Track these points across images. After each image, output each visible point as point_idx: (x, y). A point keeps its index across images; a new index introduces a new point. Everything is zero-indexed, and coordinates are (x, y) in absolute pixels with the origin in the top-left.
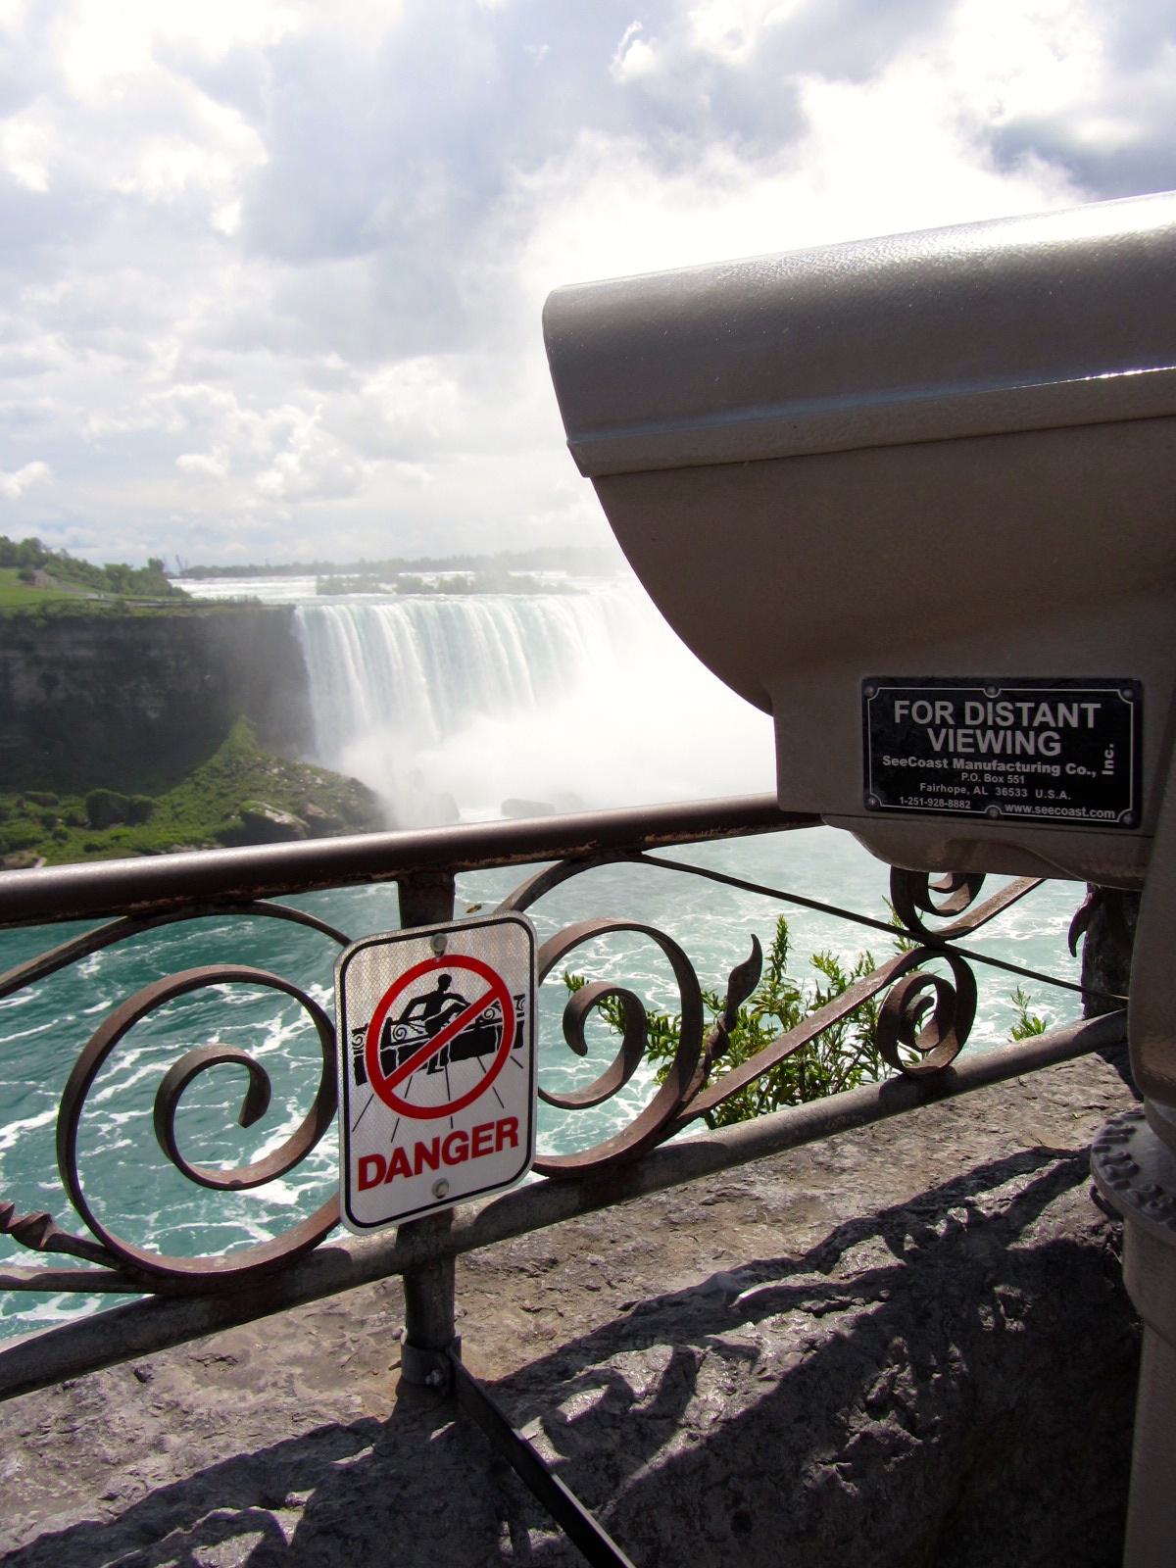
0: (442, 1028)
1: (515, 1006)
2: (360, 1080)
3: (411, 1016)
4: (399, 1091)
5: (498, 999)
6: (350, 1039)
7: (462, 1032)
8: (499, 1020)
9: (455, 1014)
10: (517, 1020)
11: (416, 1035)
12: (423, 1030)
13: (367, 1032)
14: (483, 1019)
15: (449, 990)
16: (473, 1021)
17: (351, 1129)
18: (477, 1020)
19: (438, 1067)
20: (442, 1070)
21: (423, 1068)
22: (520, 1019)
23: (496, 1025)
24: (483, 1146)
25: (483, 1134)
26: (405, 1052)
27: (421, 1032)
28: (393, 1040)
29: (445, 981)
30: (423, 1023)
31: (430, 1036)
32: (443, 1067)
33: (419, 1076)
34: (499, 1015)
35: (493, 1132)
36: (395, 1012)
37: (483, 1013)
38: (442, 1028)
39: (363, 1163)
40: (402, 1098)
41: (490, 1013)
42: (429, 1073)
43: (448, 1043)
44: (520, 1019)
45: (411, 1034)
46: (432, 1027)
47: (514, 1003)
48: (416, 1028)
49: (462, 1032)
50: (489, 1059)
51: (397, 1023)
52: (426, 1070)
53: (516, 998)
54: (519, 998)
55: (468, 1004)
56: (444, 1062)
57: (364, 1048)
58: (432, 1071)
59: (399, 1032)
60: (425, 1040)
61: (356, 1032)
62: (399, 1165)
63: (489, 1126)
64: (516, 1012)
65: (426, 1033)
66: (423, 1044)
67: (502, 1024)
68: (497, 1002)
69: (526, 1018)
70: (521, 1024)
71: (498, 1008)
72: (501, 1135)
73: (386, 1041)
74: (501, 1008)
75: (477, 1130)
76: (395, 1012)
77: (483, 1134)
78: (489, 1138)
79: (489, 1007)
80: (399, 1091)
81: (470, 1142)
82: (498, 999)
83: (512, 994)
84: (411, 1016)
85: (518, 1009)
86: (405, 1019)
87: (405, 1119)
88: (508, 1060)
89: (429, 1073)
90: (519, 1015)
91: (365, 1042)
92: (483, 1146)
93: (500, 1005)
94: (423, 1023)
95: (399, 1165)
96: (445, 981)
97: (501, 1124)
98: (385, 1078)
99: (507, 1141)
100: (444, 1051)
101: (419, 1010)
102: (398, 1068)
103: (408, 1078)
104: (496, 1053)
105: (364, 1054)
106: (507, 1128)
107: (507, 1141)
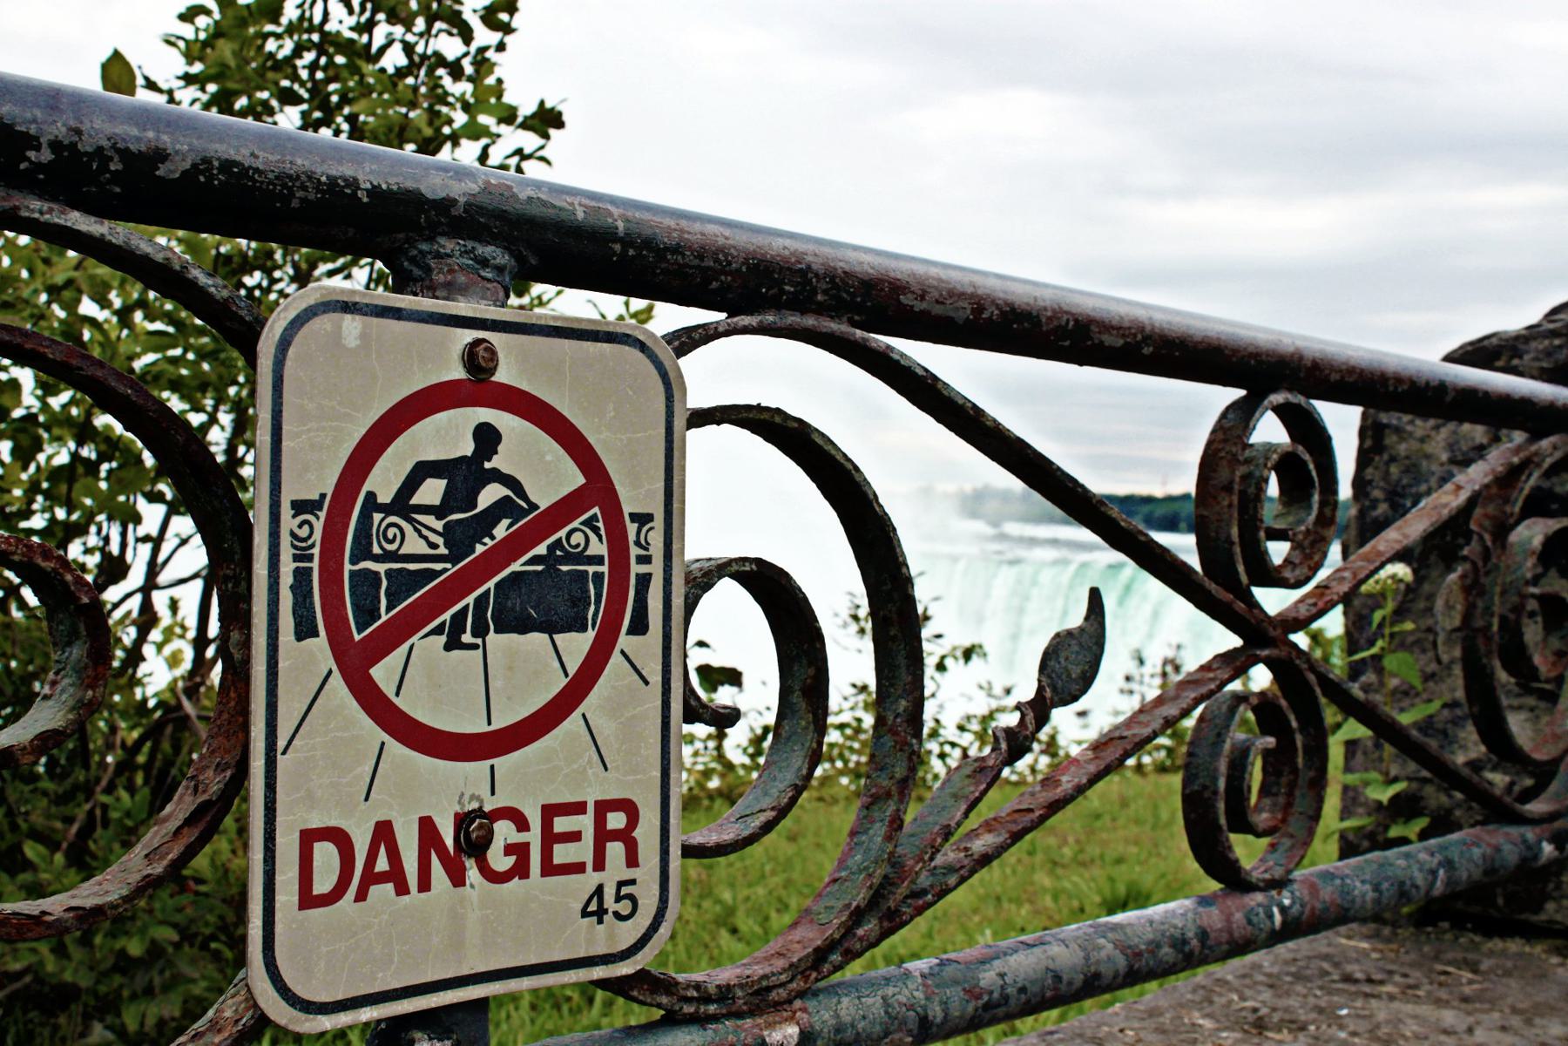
0: (480, 549)
1: (632, 537)
2: (305, 630)
3: (414, 501)
4: (383, 673)
5: (596, 510)
6: (288, 521)
7: (516, 567)
8: (598, 560)
9: (505, 522)
10: (636, 569)
11: (423, 549)
12: (440, 541)
13: (323, 514)
14: (562, 548)
15: (494, 463)
16: (541, 549)
17: (281, 744)
18: (551, 548)
19: (467, 638)
20: (475, 647)
21: (438, 631)
22: (644, 569)
23: (591, 569)
24: (562, 854)
25: (561, 824)
26: (402, 584)
27: (434, 546)
28: (376, 550)
29: (487, 438)
30: (439, 525)
31: (453, 558)
32: (479, 641)
33: (426, 646)
34: (598, 548)
35: (585, 823)
36: (384, 480)
37: (562, 533)
38: (480, 549)
39: (309, 838)
40: (389, 690)
41: (577, 538)
42: (448, 647)
43: (491, 584)
44: (644, 569)
45: (414, 545)
46: (459, 540)
47: (632, 528)
48: (425, 532)
49: (516, 567)
50: (577, 645)
51: (387, 509)
52: (443, 639)
53: (635, 518)
54: (643, 519)
55: (534, 507)
56: (480, 631)
57: (316, 551)
58: (453, 644)
59: (390, 535)
60: (438, 567)
61: (300, 507)
62: (382, 864)
63: (578, 808)
64: (634, 551)
65: (443, 550)
66: (435, 574)
67: (605, 569)
68: (594, 517)
69: (656, 569)
70: (644, 580)
71: (596, 530)
72: (603, 836)
73: (362, 551)
74: (603, 532)
75: (550, 812)
76: (384, 480)
77: (561, 824)
78: (575, 836)
79: (575, 524)
80: (383, 673)
81: (534, 837)
82: (596, 510)
83: (627, 509)
84: (414, 501)
85: (638, 543)
86: (402, 505)
87: (395, 748)
88: (616, 659)
89: (448, 647)
90: (645, 560)
91: (317, 536)
92: (562, 854)
93: (600, 525)
94: (439, 525)
95: (382, 864)
96: (487, 438)
97: (603, 808)
98: (357, 637)
99: (615, 850)
100: (481, 602)
101: (432, 491)
102: (384, 618)
103: (406, 646)
104: (591, 634)
105: (315, 565)
106: (616, 821)
107: (615, 850)
